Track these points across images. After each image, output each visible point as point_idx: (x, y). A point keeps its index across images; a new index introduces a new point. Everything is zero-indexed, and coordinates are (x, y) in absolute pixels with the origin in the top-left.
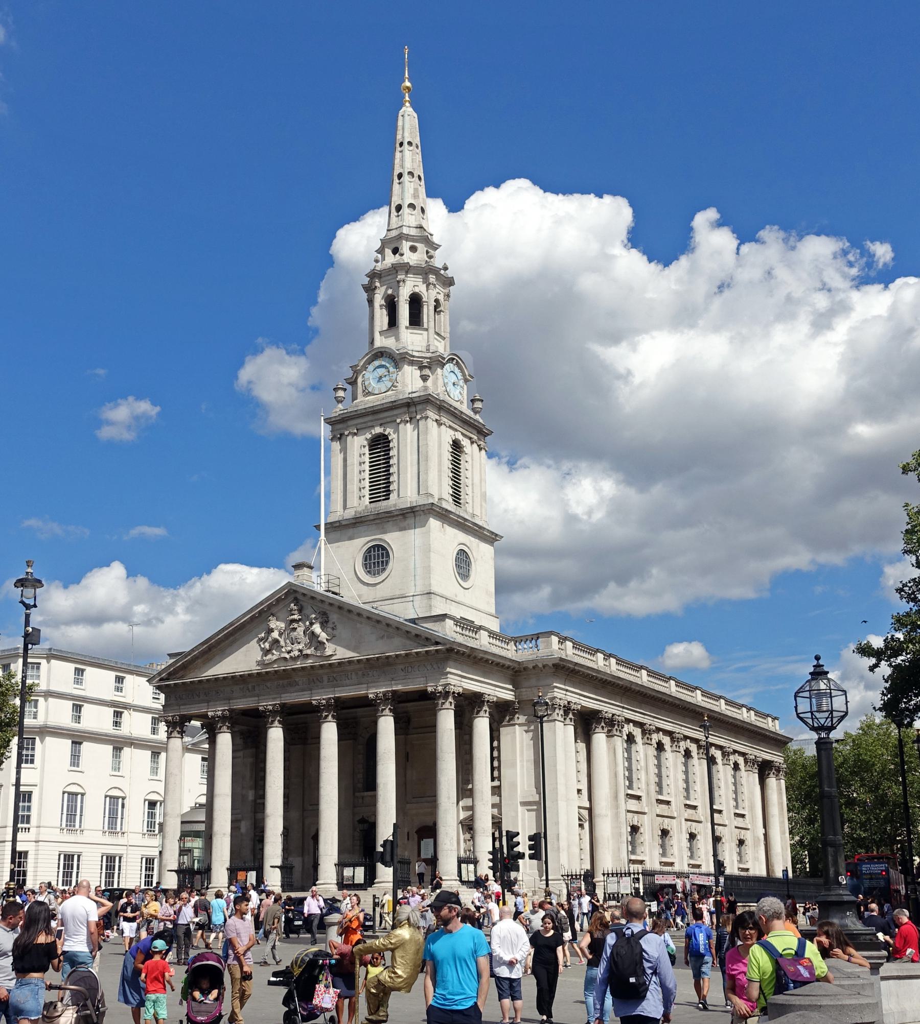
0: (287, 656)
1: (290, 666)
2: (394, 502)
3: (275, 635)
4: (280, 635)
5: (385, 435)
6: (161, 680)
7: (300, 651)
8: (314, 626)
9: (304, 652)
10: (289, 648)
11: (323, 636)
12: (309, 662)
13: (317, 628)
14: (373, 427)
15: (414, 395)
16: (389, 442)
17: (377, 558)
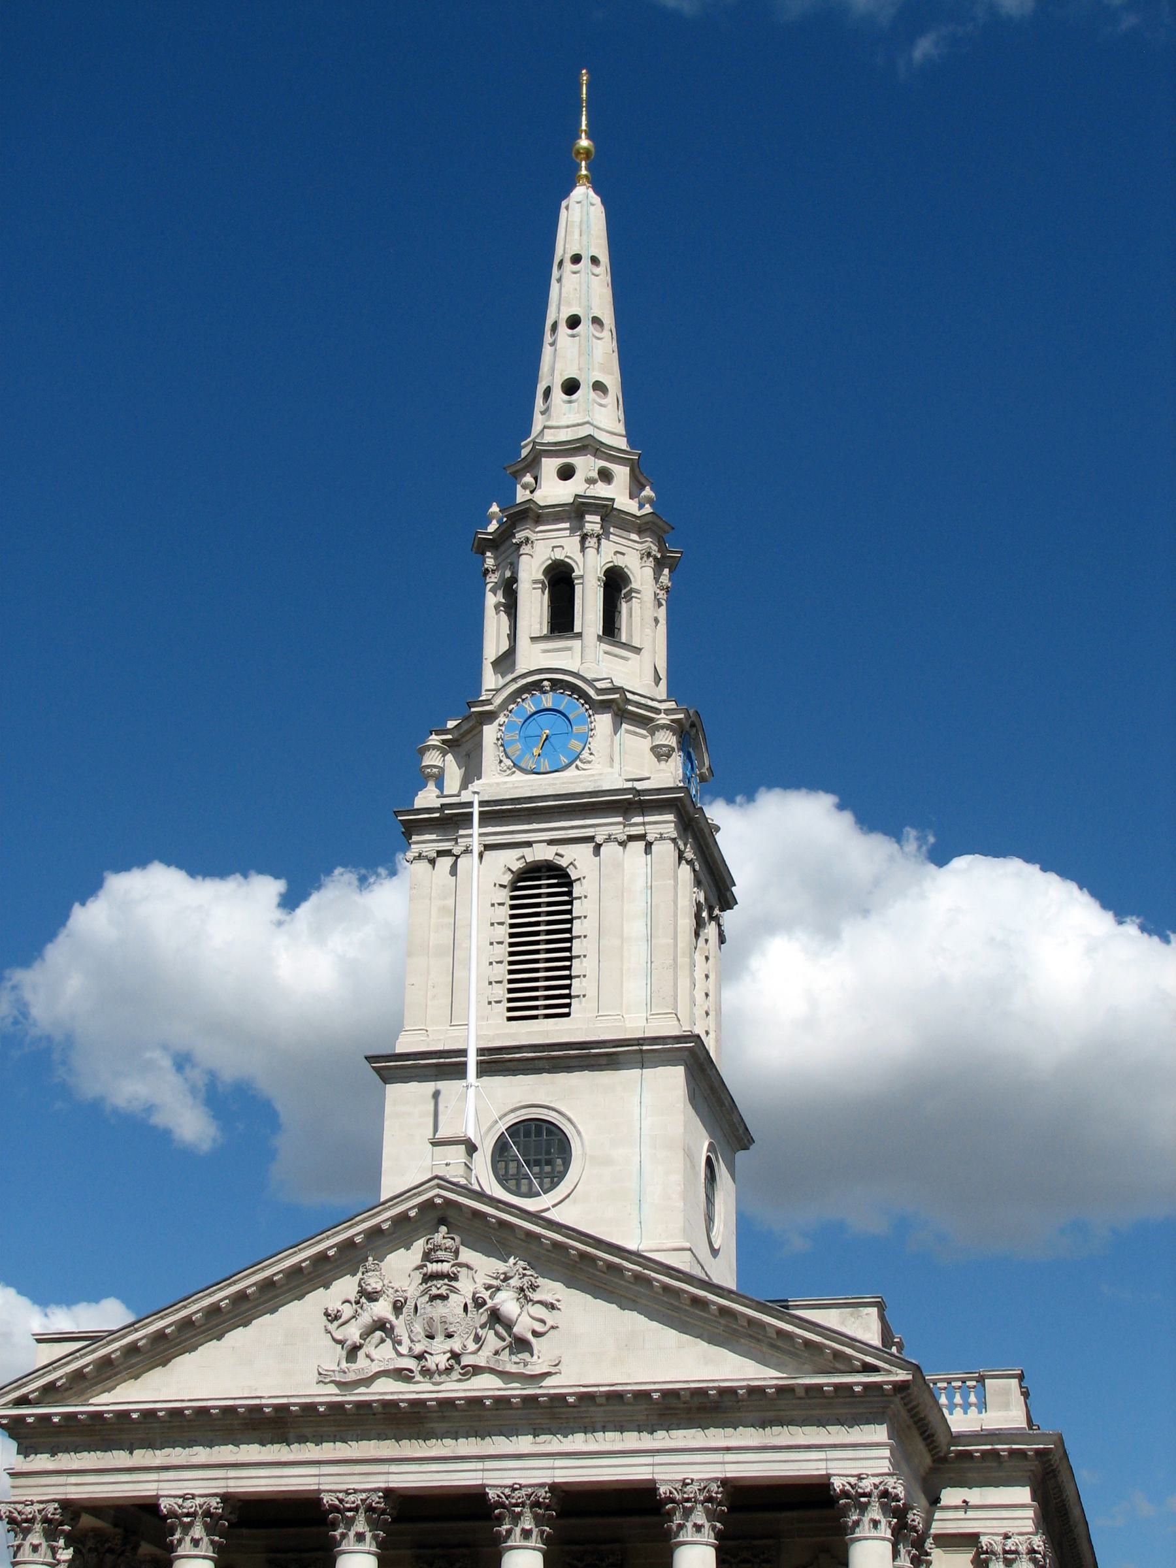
0: (411, 1364)
1: (421, 1389)
2: (579, 1026)
3: (382, 1309)
4: (398, 1308)
5: (559, 868)
6: (22, 1401)
7: (456, 1356)
8: (501, 1296)
9: (465, 1360)
10: (418, 1349)
11: (523, 1327)
12: (486, 1385)
13: (507, 1303)
14: (529, 844)
15: (639, 786)
16: (570, 884)
17: (538, 1148)
